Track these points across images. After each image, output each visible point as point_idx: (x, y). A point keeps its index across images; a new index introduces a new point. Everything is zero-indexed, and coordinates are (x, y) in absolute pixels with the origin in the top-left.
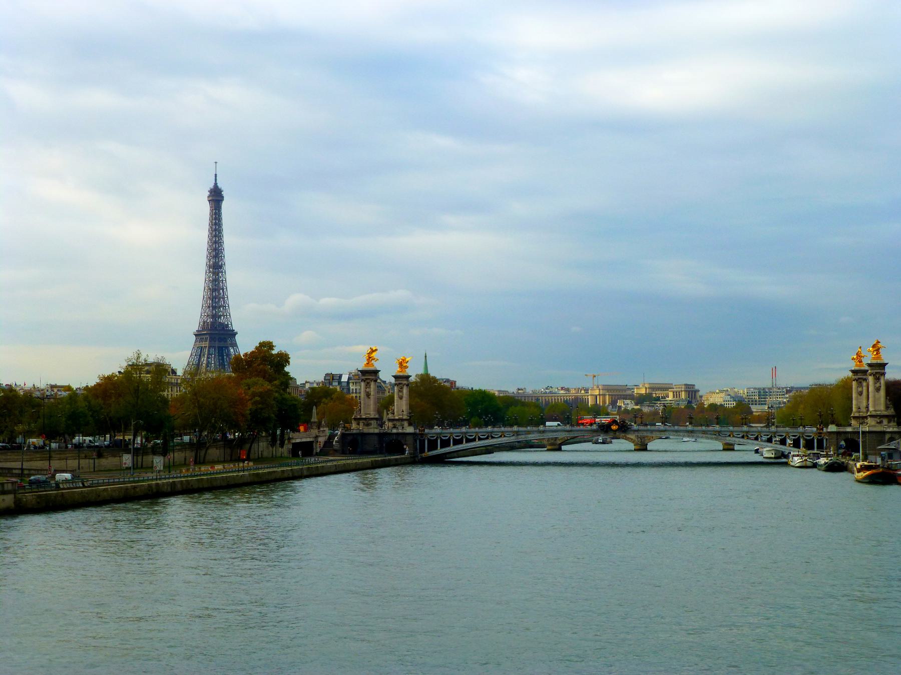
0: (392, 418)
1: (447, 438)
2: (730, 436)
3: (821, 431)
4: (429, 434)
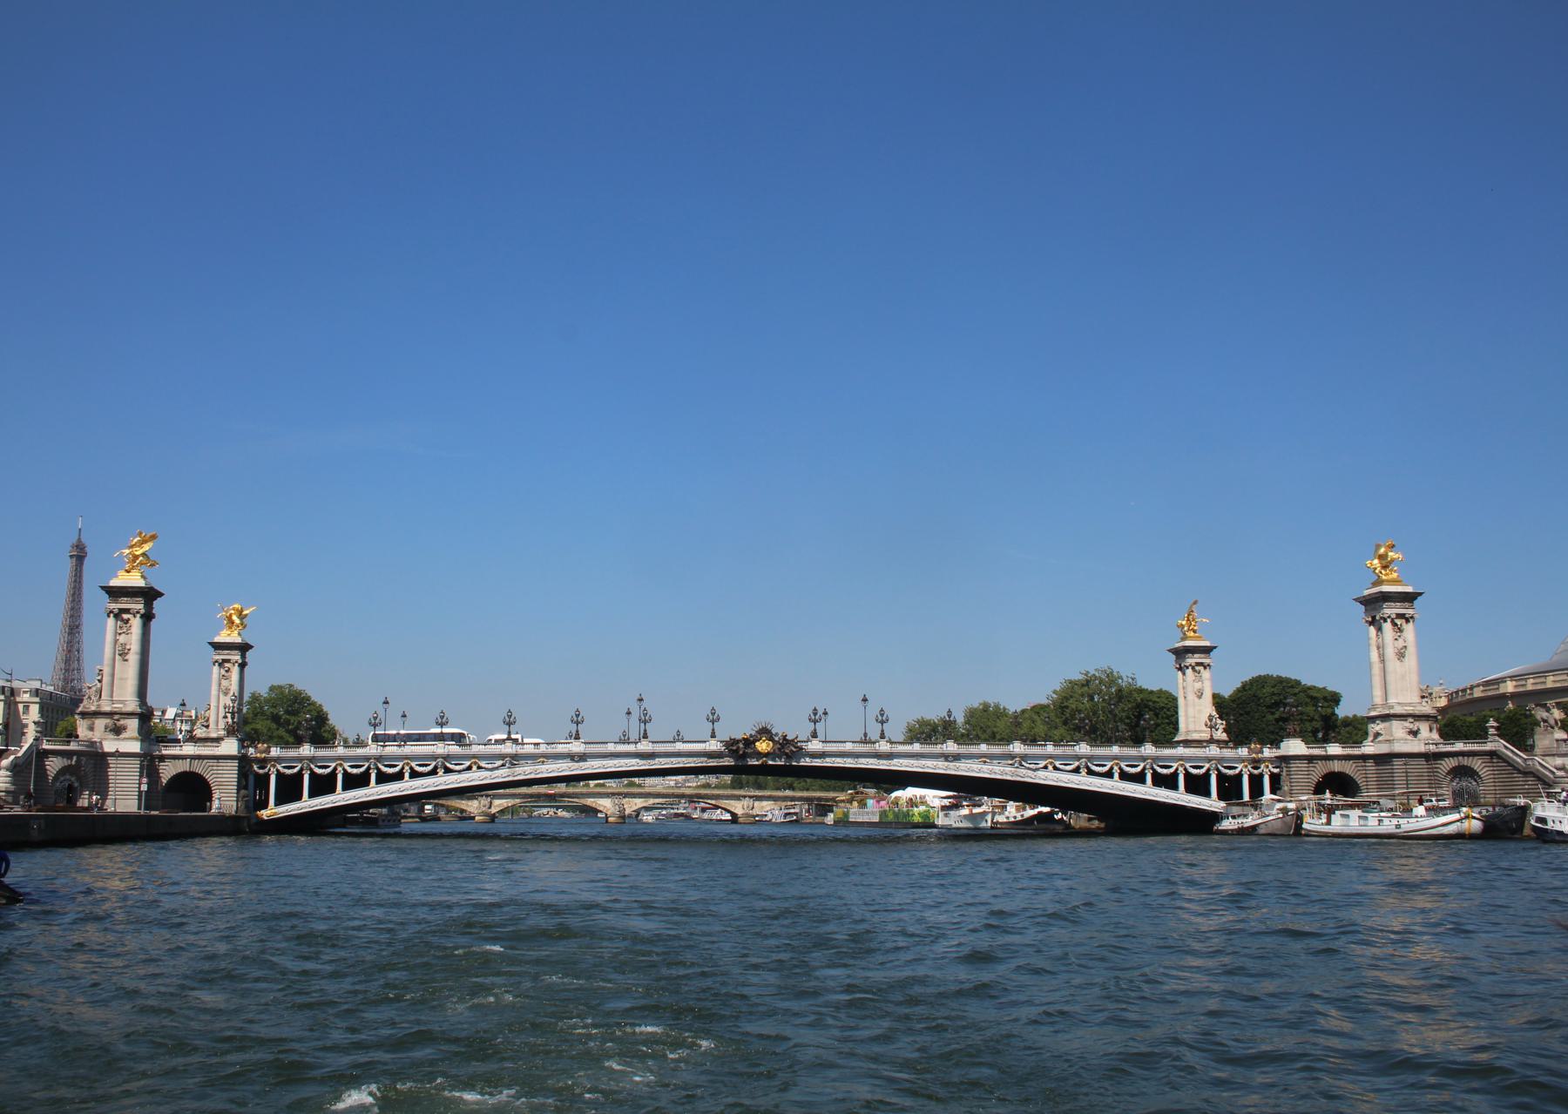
0: (203, 735)
1: (329, 770)
2: (1046, 767)
3: (1260, 755)
4: (278, 760)
